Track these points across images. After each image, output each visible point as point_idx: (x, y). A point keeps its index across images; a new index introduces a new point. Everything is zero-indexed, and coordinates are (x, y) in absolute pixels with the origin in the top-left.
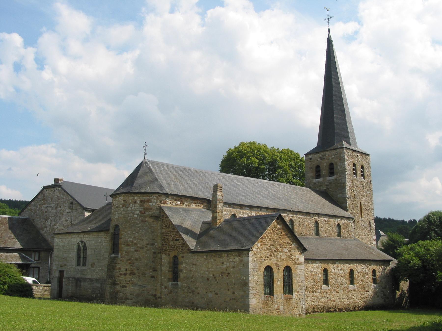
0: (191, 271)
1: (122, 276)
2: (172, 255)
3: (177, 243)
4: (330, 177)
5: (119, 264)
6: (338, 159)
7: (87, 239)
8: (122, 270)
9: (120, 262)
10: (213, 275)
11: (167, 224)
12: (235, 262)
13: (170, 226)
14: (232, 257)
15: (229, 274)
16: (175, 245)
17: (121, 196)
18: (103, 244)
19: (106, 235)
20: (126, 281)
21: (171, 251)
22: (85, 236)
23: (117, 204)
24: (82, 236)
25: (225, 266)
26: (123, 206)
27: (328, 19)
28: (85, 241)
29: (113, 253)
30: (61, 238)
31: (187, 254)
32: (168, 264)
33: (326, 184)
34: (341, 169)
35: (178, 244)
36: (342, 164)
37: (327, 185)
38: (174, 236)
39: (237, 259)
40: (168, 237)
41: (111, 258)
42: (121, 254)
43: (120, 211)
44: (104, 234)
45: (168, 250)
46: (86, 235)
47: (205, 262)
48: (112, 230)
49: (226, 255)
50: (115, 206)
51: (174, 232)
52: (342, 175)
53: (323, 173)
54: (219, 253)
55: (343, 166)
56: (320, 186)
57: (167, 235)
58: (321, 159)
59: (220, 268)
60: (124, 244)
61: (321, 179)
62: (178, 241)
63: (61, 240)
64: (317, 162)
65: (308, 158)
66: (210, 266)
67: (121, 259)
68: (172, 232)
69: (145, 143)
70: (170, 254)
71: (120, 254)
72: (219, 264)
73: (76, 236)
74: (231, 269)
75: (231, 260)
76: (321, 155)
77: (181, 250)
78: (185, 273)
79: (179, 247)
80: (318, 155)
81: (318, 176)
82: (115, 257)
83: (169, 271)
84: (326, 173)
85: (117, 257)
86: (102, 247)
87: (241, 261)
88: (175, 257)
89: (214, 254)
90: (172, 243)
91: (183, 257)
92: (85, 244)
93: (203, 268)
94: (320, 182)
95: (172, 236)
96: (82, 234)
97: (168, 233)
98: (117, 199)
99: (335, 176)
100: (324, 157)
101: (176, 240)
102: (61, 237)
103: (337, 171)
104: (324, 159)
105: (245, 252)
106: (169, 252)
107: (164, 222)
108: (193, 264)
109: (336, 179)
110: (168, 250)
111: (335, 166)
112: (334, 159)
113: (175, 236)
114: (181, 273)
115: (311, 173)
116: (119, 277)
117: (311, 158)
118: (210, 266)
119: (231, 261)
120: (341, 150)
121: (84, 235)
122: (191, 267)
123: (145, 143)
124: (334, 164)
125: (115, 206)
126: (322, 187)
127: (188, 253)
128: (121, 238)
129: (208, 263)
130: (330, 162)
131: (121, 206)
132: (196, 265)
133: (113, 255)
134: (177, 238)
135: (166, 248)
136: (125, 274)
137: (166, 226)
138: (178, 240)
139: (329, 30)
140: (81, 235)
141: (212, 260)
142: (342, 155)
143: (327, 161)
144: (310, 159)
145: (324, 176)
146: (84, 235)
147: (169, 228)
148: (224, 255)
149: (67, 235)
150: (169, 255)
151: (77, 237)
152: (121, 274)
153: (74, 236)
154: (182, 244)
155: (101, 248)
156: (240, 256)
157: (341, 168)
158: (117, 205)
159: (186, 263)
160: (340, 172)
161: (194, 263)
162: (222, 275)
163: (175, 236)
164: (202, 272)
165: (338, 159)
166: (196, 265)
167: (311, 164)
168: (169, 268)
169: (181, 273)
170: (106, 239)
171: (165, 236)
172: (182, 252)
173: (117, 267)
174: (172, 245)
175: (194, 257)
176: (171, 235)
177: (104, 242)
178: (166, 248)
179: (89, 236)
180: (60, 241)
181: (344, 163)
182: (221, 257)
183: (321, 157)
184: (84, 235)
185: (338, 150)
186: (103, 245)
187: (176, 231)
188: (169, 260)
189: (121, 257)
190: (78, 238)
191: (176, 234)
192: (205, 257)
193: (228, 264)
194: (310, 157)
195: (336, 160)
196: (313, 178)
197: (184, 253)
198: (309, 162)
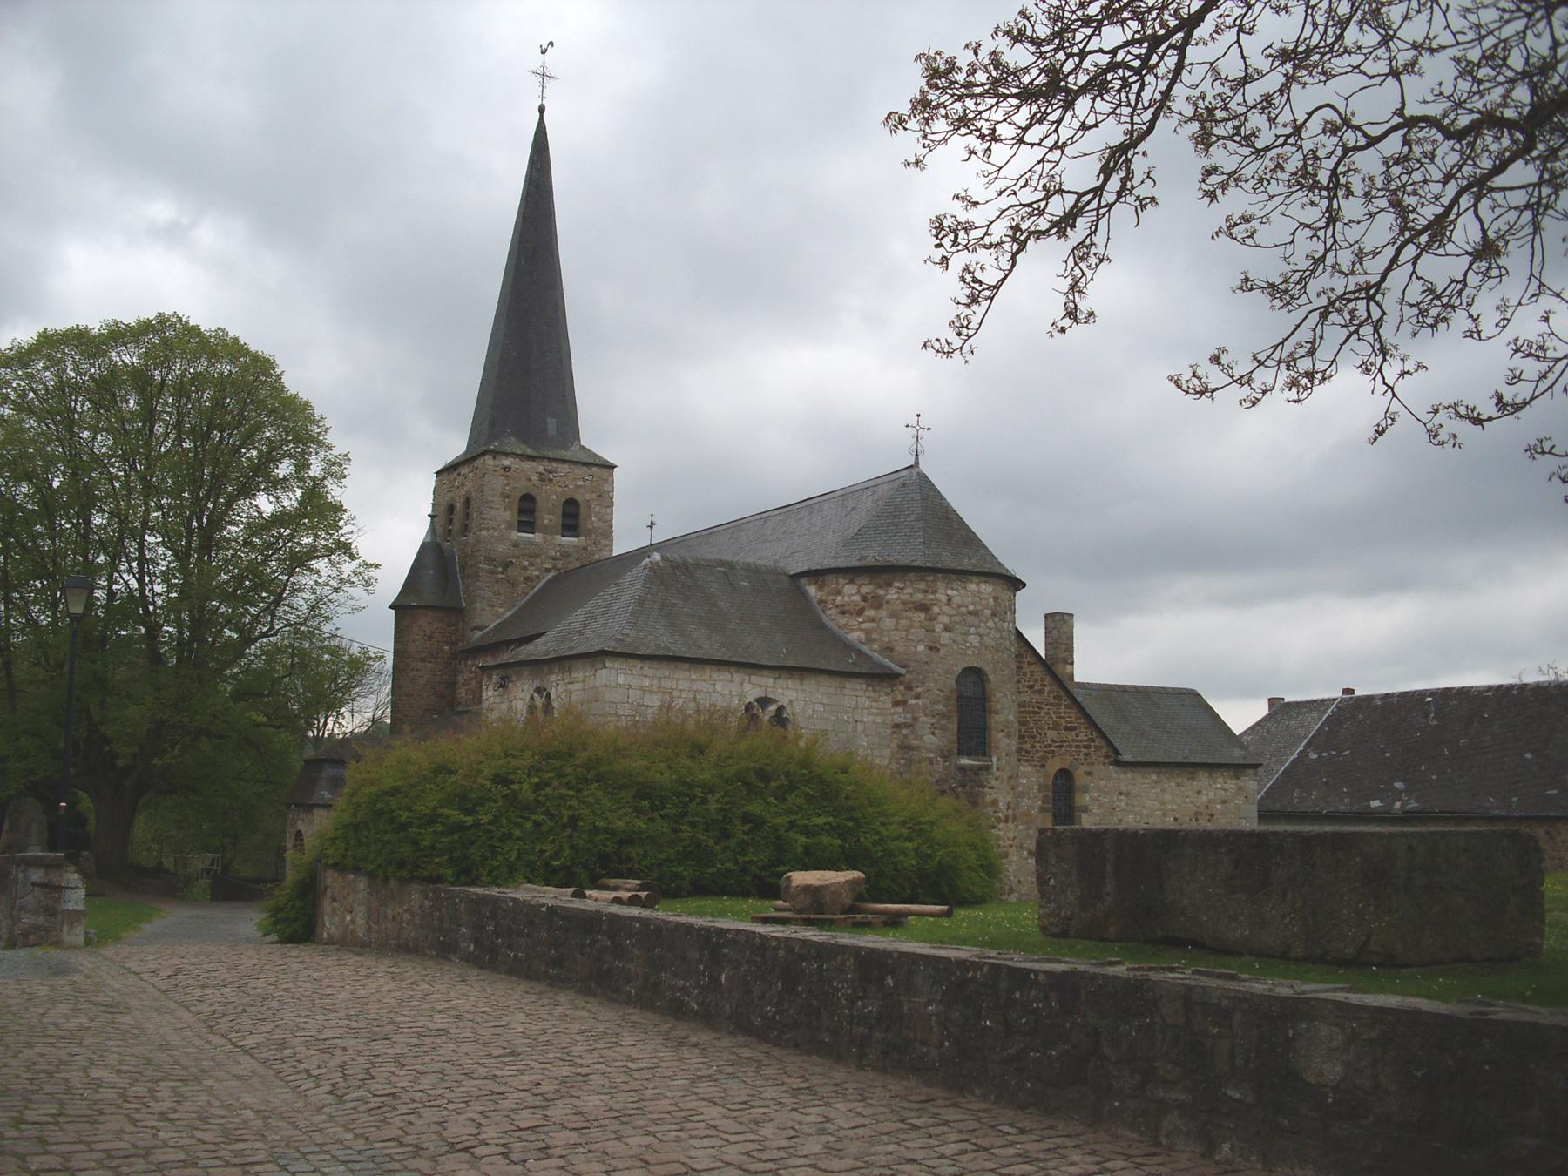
0: (1114, 809)
1: (1001, 825)
2: (1054, 765)
3: (1071, 736)
4: (564, 538)
5: (992, 788)
6: (594, 496)
7: (792, 695)
8: (1001, 805)
9: (994, 783)
10: (1176, 819)
11: (1036, 681)
12: (1226, 790)
13: (1047, 689)
14: (1221, 780)
15: (1212, 815)
16: (1064, 741)
17: (985, 582)
18: (865, 720)
19: (875, 691)
20: (1008, 839)
21: (1050, 756)
22: (780, 682)
23: (973, 603)
24: (770, 681)
25: (1204, 798)
26: (994, 614)
27: (546, 79)
28: (784, 701)
29: (961, 753)
30: (646, 676)
31: (1103, 767)
32: (1040, 791)
33: (552, 553)
34: (600, 524)
35: (1074, 740)
36: (604, 511)
37: (553, 558)
38: (1060, 717)
39: (1231, 784)
40: (1037, 717)
41: (962, 769)
42: (998, 760)
43: (988, 627)
44: (864, 686)
45: (1040, 754)
46: (788, 679)
47: (1153, 788)
48: (939, 683)
49: (1206, 774)
50: (959, 607)
51: (1061, 705)
52: (604, 542)
53: (546, 522)
54: (1192, 769)
55: (608, 517)
56: (532, 556)
57: (1034, 712)
58: (542, 480)
59: (1192, 802)
60: (1002, 731)
61: (537, 537)
62: (1074, 733)
63: (647, 683)
64: (529, 484)
65: (497, 463)
66: (1168, 797)
67: (998, 773)
68: (1052, 705)
69: (918, 416)
70: (1047, 765)
71: (994, 759)
72: (1190, 794)
73: (737, 677)
74: (1218, 806)
75: (1219, 786)
76: (541, 469)
77: (1082, 757)
78: (1098, 814)
79: (1077, 747)
80: (534, 464)
81: (527, 524)
82: (980, 768)
83: (1042, 810)
84: (552, 524)
85: (988, 768)
86: (860, 727)
87: (1240, 789)
88: (1065, 775)
89: (1177, 771)
90: (1052, 734)
91: (1089, 774)
92: (781, 709)
93: (1149, 803)
94: (531, 543)
95: (1054, 716)
96: (765, 673)
97: (1038, 707)
98: (972, 587)
99: (582, 538)
100: (551, 476)
101: (1066, 728)
102: (650, 672)
103: (589, 526)
104: (551, 480)
105: (1250, 771)
106: (1043, 758)
107: (1025, 674)
108: (1121, 794)
109: (585, 549)
110: (1040, 754)
111: (583, 511)
112: (582, 491)
113: (1064, 718)
114: (1083, 815)
115: (505, 509)
116: (994, 827)
117: (510, 468)
118: (1168, 797)
119: (1217, 788)
120: (605, 472)
121: (775, 679)
122: (1115, 799)
123: (918, 416)
124: (582, 505)
125: (959, 607)
126: (538, 560)
127: (1104, 764)
128: (997, 713)
129: (1163, 790)
130: (568, 497)
131: (987, 612)
132: (1127, 794)
133: (965, 761)
134: (1067, 722)
135: (1033, 747)
136: (1006, 820)
137: (1031, 687)
138: (1074, 728)
139: (542, 110)
140: (762, 676)
141: (1173, 784)
142: (606, 487)
143: (560, 489)
144: (505, 468)
145: (545, 530)
146: (779, 677)
147: (1041, 692)
148: (1203, 775)
149: (686, 666)
150: (1043, 766)
151: (742, 684)
152: (999, 820)
153: (725, 676)
154: (1085, 741)
155: (855, 730)
156: (1237, 778)
157: (600, 520)
158: (971, 608)
159: (1099, 790)
160: (600, 531)
161: (1124, 789)
162: (1197, 820)
163: (1064, 718)
164: (1145, 812)
165: (594, 496)
166: (1127, 794)
167: (508, 485)
168: (1043, 802)
169: (1083, 815)
170: (874, 704)
171: (1029, 712)
172: (1086, 759)
173: (988, 799)
174: (1053, 741)
175: (1122, 776)
176: (1048, 713)
177: (868, 714)
178: (1033, 747)
179: (801, 684)
180: (642, 689)
181: (609, 510)
182: (1193, 779)
183: (541, 474)
184: (775, 679)
185: (594, 469)
186: (861, 722)
187: (1065, 706)
188: (1042, 780)
189: (998, 769)
190: (747, 687)
191: (1065, 713)
192: (1154, 777)
193: (1211, 795)
194: (507, 462)
195: (588, 496)
196: (510, 527)
197: (1093, 764)
198: (502, 476)
